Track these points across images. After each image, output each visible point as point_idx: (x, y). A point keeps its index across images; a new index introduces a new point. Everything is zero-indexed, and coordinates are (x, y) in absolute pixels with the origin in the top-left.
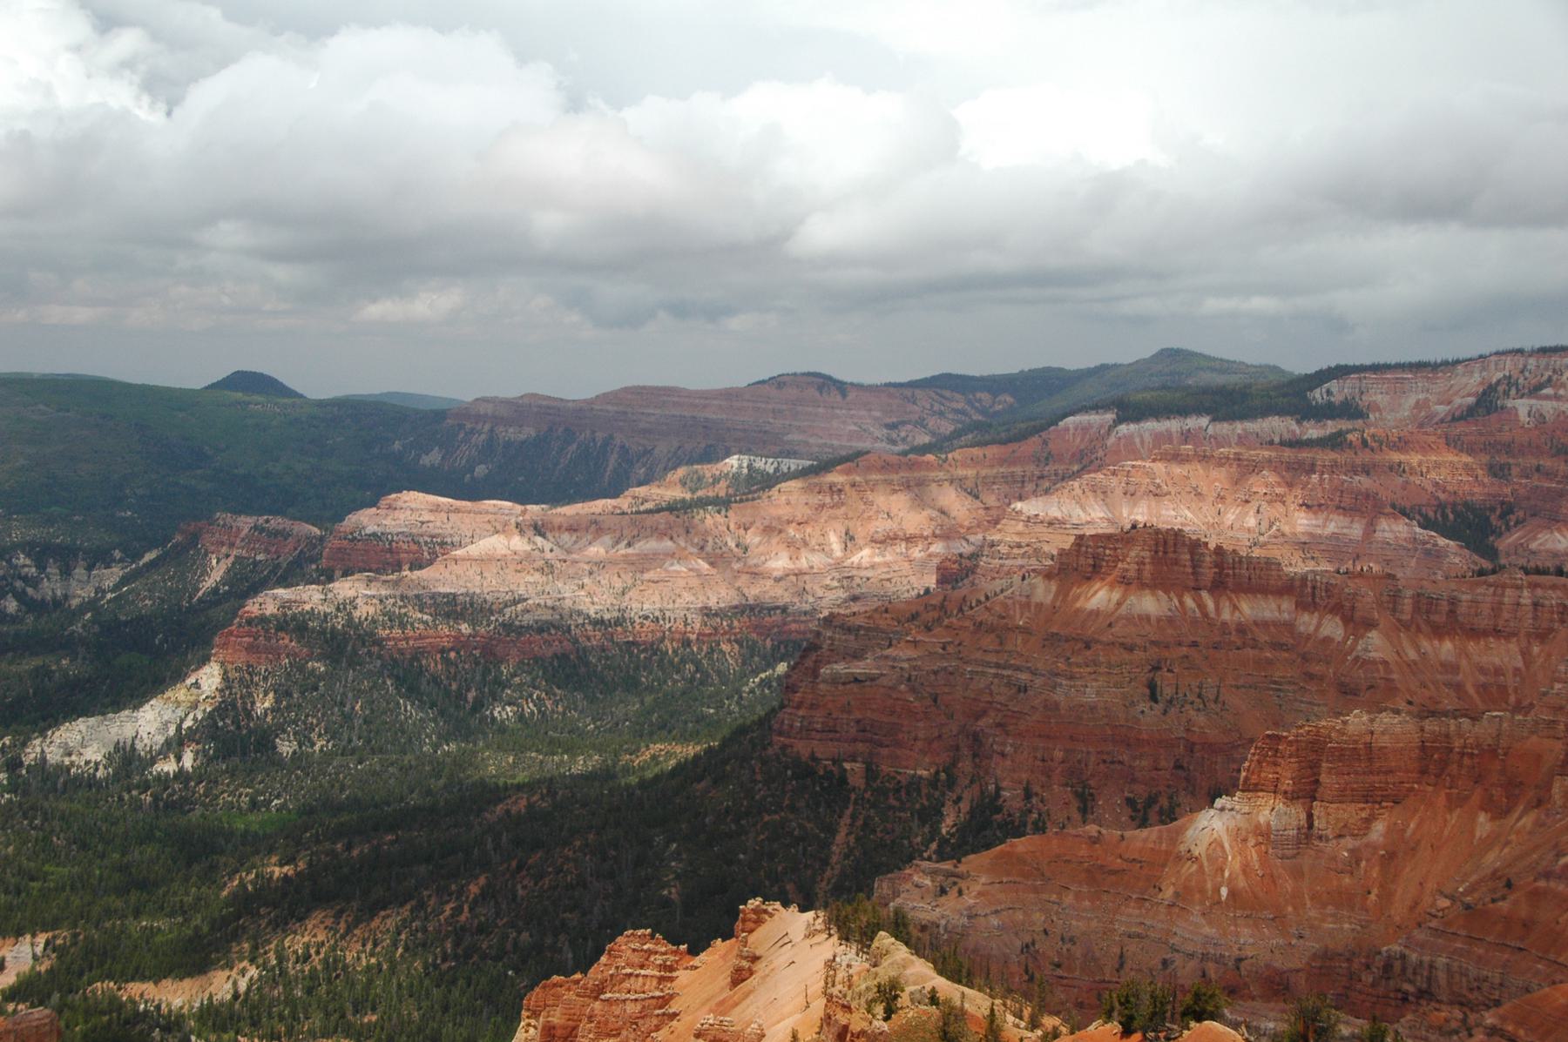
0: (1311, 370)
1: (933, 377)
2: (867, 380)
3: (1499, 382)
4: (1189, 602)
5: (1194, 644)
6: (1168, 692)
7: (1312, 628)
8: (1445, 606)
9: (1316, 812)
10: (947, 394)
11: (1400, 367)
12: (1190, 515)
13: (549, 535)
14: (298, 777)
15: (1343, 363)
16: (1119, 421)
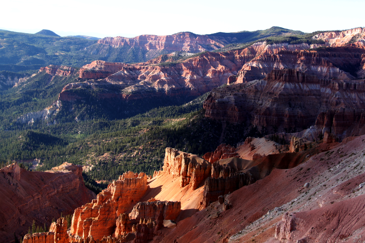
0: (311, 32)
1: (217, 33)
2: (201, 34)
3: (356, 35)
4: (297, 85)
5: (298, 95)
6: (293, 105)
7: (324, 91)
8: (353, 86)
9: (332, 129)
10: (221, 37)
11: (333, 31)
12: (287, 67)
13: (133, 71)
14: (85, 126)
15: (319, 30)
16: (267, 44)
